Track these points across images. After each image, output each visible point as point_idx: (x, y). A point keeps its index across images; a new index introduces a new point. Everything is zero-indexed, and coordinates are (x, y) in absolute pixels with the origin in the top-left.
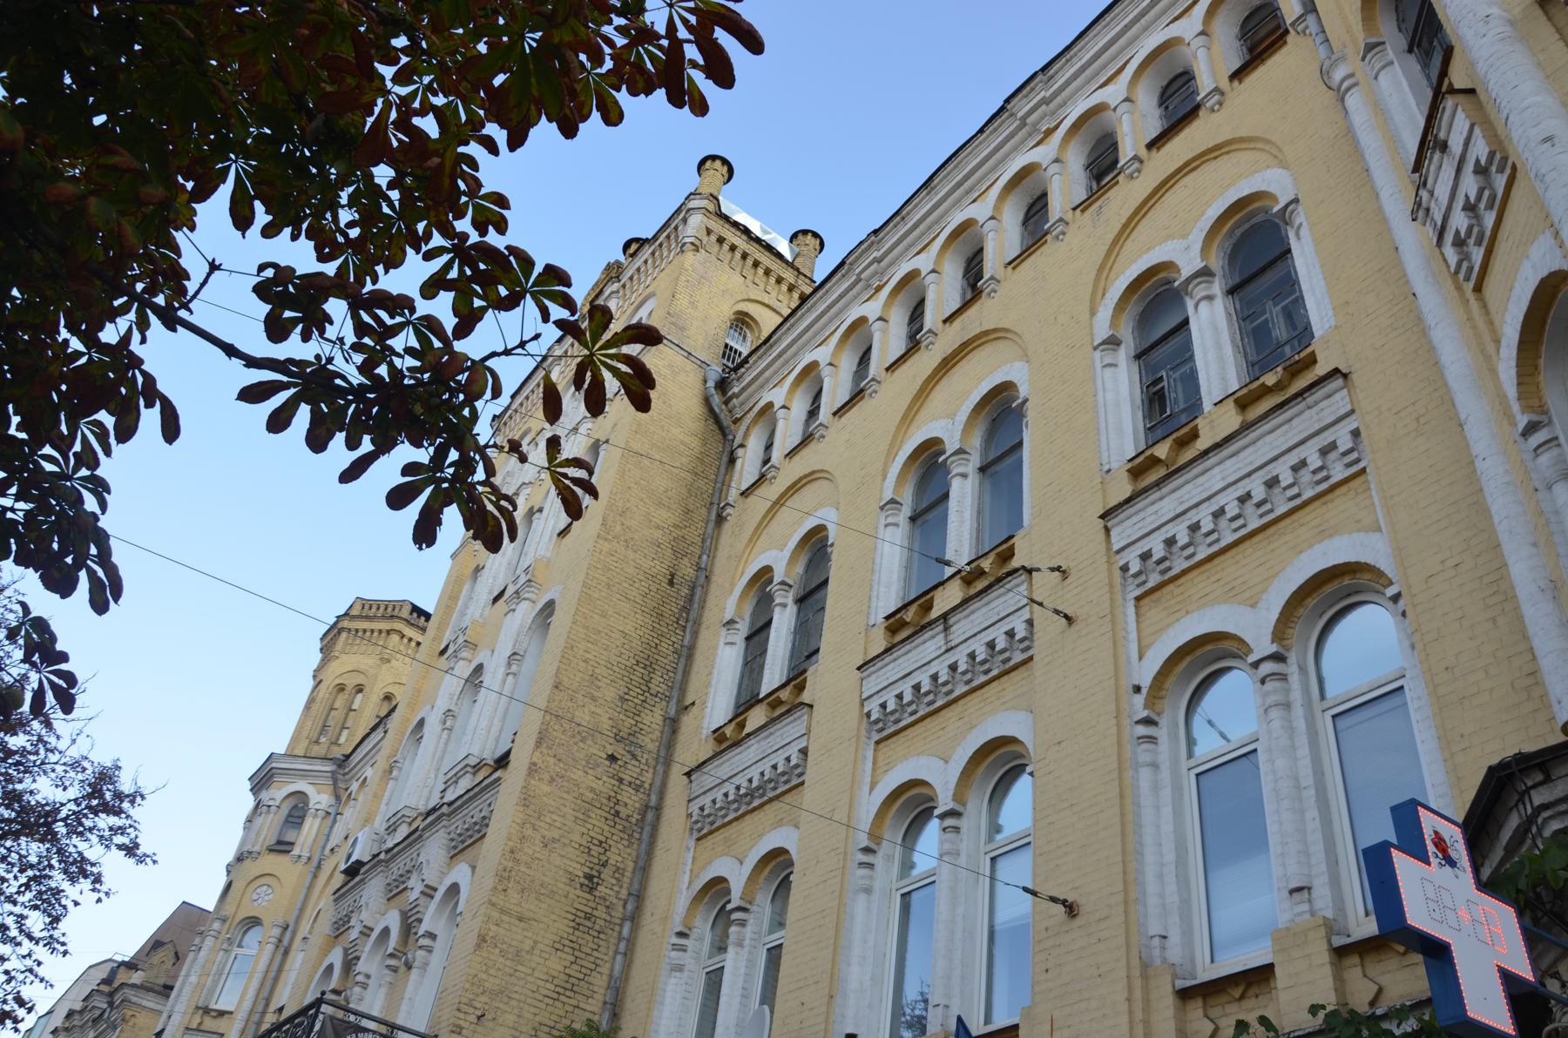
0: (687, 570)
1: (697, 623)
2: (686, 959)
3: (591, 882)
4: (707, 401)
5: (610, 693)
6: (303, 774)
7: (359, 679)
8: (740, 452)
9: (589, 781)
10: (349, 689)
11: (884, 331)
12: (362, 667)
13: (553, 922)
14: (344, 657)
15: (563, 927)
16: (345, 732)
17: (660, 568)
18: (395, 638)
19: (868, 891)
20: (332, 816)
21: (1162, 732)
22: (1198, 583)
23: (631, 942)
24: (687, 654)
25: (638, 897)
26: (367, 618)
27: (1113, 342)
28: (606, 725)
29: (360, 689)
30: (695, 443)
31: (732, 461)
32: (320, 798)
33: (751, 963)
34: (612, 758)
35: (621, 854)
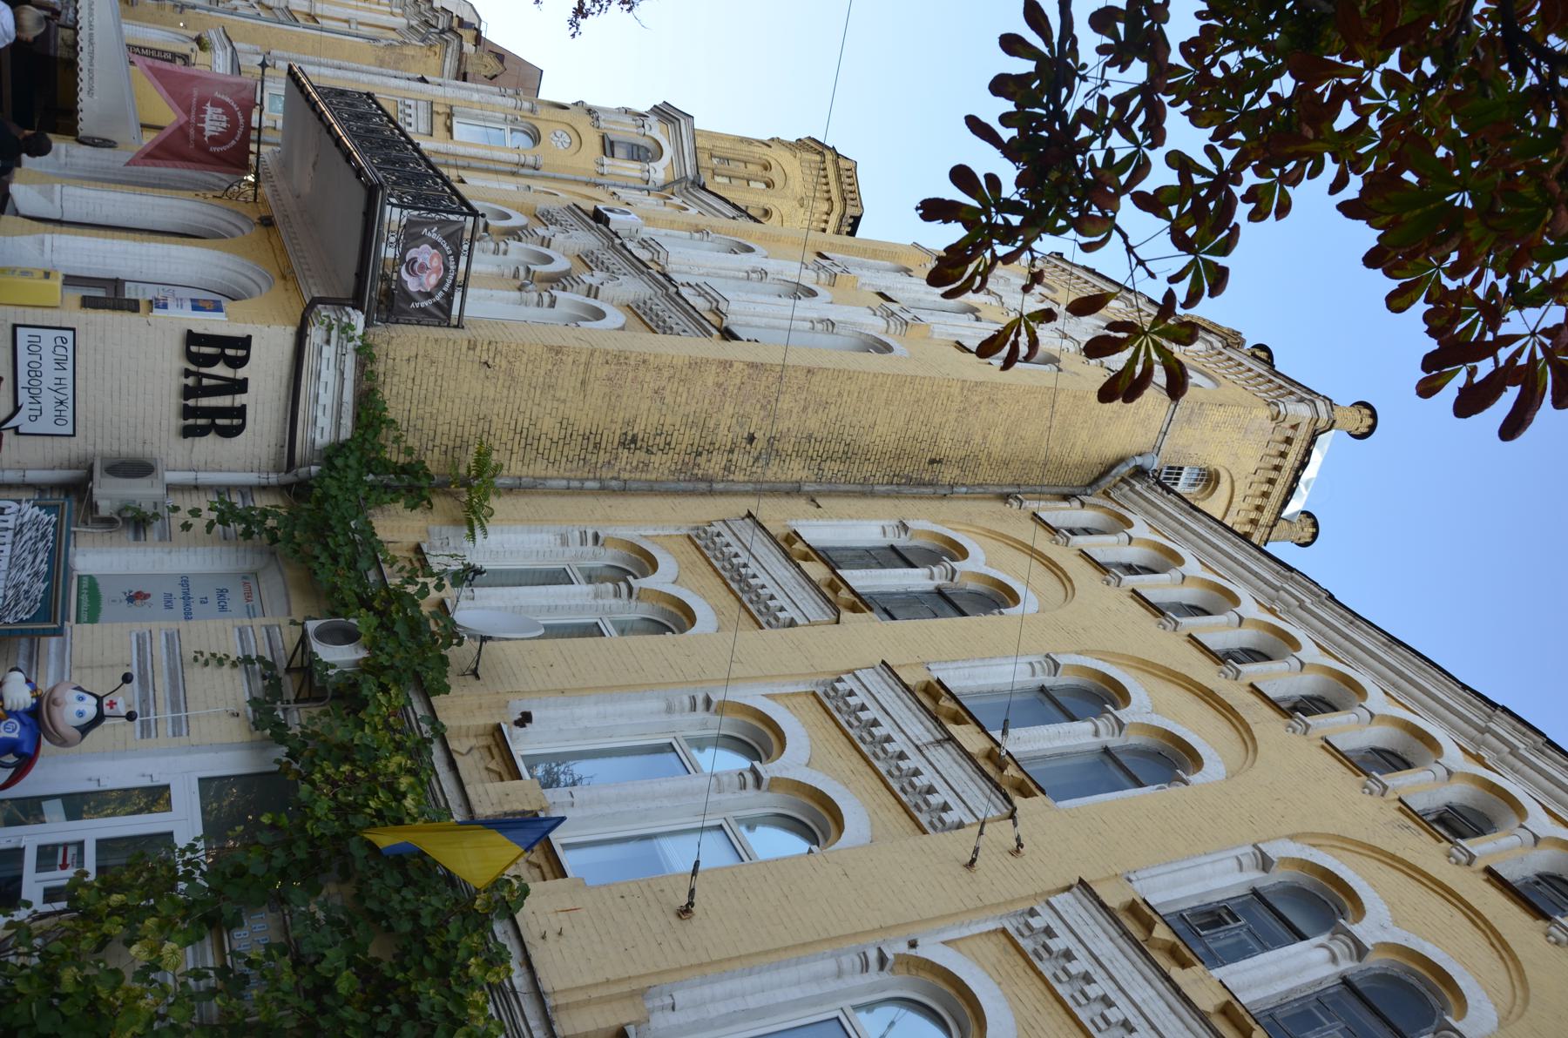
0: (948, 474)
1: (898, 495)
2: (574, 547)
3: (630, 442)
4: (1121, 460)
5: (813, 423)
6: (679, 151)
7: (779, 183)
8: (1076, 504)
9: (725, 422)
10: (768, 174)
11: (1229, 625)
12: (791, 182)
13: (587, 413)
14: (797, 163)
15: (584, 425)
16: (726, 180)
17: (945, 448)
18: (825, 207)
19: (669, 710)
20: (646, 186)
21: (874, 976)
22: (1031, 990)
23: (581, 491)
24: (865, 491)
25: (625, 490)
26: (839, 176)
27: (1265, 863)
28: (782, 426)
30: (1076, 457)
31: (1065, 498)
32: (660, 171)
33: (581, 609)
34: (751, 439)
35: (661, 466)
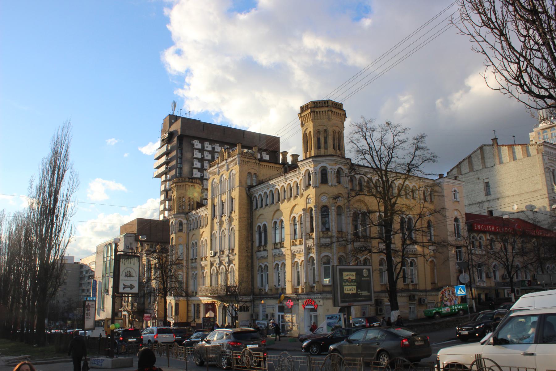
0: (250, 221)
3: (247, 265)
5: (244, 243)
6: (180, 217)
7: (182, 196)
29: (183, 197)
30: (246, 201)
32: (184, 221)
